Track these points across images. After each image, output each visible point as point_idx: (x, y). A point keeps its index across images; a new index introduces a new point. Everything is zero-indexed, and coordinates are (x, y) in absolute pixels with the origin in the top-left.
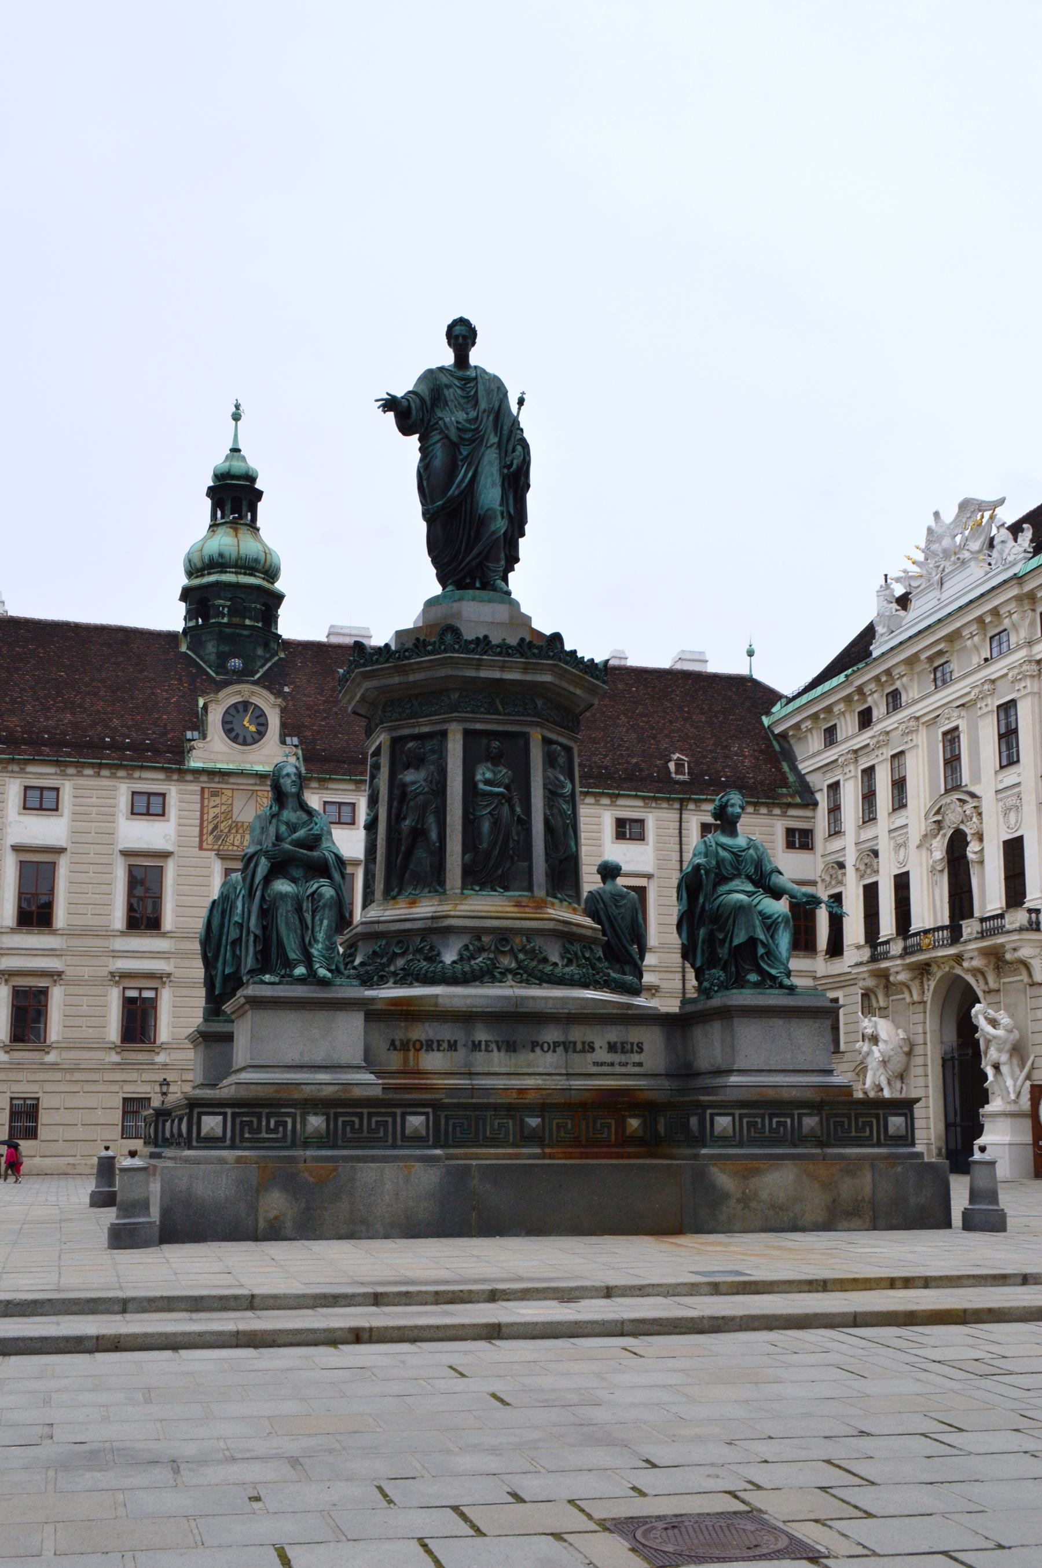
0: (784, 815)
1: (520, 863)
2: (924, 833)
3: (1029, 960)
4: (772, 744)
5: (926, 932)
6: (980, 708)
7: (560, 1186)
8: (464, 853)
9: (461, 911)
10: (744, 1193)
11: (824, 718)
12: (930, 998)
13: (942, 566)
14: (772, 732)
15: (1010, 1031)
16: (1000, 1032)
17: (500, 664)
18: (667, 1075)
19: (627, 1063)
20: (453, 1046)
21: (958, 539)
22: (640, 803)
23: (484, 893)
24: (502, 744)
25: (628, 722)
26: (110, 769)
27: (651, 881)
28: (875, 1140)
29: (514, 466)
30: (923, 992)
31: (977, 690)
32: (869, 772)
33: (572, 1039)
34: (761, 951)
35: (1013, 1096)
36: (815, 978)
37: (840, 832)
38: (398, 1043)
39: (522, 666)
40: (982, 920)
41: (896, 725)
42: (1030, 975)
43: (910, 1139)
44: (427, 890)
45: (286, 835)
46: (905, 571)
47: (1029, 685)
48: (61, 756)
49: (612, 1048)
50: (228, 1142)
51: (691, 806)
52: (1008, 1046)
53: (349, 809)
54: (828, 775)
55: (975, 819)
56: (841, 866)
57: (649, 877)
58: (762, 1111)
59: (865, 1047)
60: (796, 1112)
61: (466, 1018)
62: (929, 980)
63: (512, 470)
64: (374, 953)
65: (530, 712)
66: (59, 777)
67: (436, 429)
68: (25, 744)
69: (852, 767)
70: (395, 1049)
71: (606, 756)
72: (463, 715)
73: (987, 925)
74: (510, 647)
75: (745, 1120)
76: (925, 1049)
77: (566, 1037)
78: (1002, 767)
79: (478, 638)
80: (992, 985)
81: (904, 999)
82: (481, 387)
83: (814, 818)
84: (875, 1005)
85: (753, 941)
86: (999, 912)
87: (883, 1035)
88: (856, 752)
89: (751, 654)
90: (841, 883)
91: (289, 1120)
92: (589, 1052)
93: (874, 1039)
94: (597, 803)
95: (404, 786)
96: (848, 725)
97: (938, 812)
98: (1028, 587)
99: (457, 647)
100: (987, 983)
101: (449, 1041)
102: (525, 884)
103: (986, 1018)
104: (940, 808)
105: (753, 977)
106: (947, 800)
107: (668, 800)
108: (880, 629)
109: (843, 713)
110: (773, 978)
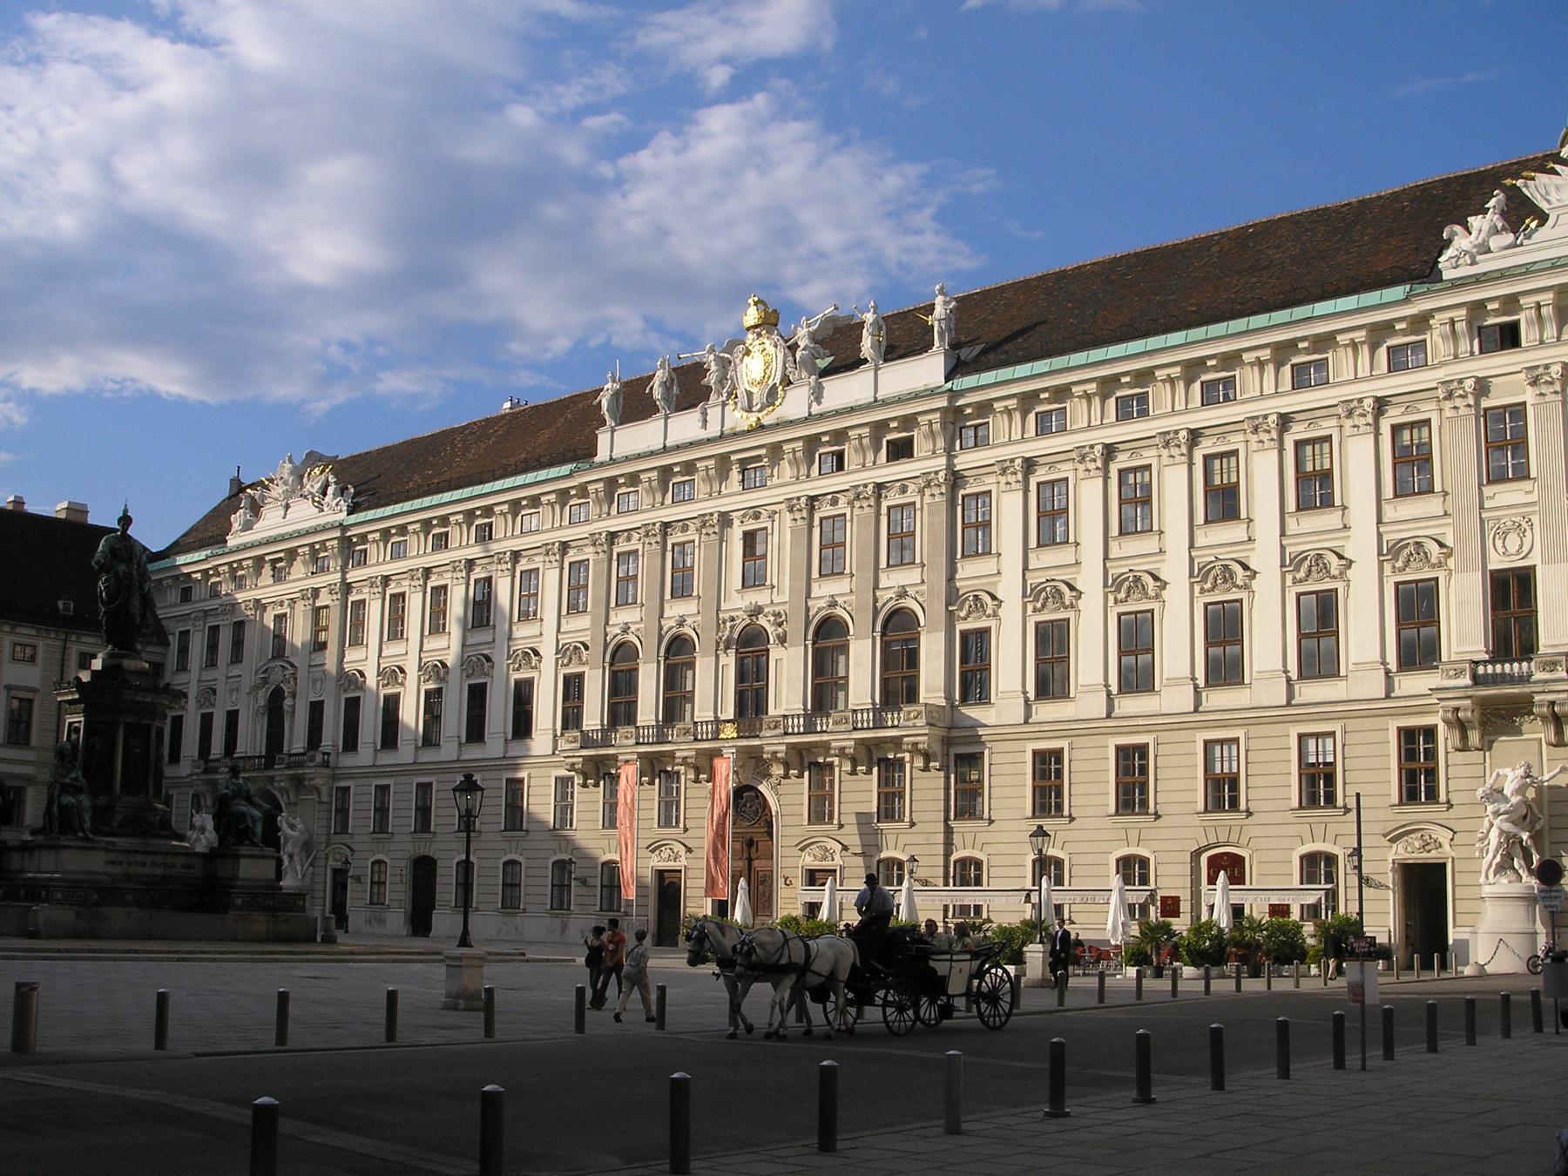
20: (121, 864)
22: (33, 632)
27: (37, 695)
32: (214, 630)
35: (300, 877)
42: (320, 797)
49: (183, 866)
51: (73, 638)
52: (301, 843)
54: (182, 623)
55: (292, 682)
78: (314, 650)
86: (302, 751)
88: (205, 612)
90: (183, 708)
93: (203, 830)
100: (289, 798)
103: (287, 823)
105: (247, 842)
106: (272, 664)
108: (236, 526)
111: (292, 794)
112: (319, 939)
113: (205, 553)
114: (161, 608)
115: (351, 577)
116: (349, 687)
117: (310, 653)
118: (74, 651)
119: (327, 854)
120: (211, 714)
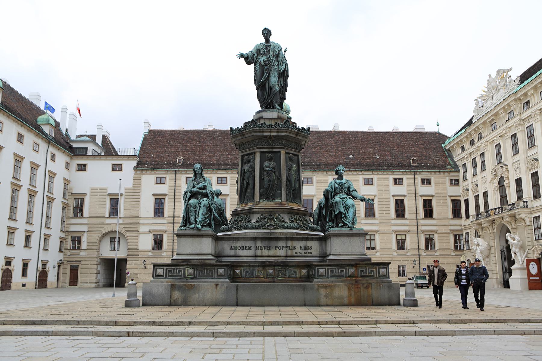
0: (449, 175)
1: (278, 191)
2: (491, 178)
3: (524, 218)
4: (445, 153)
5: (492, 210)
6: (506, 137)
7: (265, 291)
8: (260, 189)
9: (258, 207)
10: (326, 293)
11: (460, 143)
12: (495, 232)
13: (492, 92)
14: (445, 149)
15: (519, 241)
16: (516, 242)
17: (269, 130)
18: (320, 257)
19: (307, 253)
20: (250, 248)
21: (497, 82)
22: (401, 173)
23: (266, 201)
24: (272, 155)
25: (398, 149)
26: (231, 171)
27: (406, 198)
28: (375, 276)
29: (282, 70)
30: (493, 230)
31: (504, 131)
32: (474, 159)
33: (288, 246)
34: (343, 216)
35: (521, 263)
36: (461, 226)
37: (467, 179)
38: (233, 247)
39: (276, 131)
40: (509, 205)
41: (481, 144)
43: (388, 276)
44: (250, 201)
45: (196, 185)
46: (481, 95)
47: (520, 128)
48: (227, 168)
50: (165, 277)
51: (418, 173)
52: (518, 246)
53: (311, 179)
54: (463, 162)
55: (506, 173)
56: (468, 190)
57: (405, 196)
58: (335, 267)
59: (475, 248)
60: (347, 267)
61: (255, 239)
62: (495, 225)
63: (281, 71)
64: (235, 220)
65: (281, 144)
66: (227, 174)
67: (258, 62)
68: (217, 165)
69: (469, 159)
70: (232, 249)
71: (390, 159)
72: (260, 147)
73: (512, 206)
74: (272, 125)
75: (329, 270)
76: (495, 248)
77: (286, 245)
79: (262, 123)
80: (514, 227)
81: (487, 232)
82: (272, 48)
83: (459, 175)
84: (479, 234)
85: (340, 213)
87: (481, 244)
88: (470, 153)
89: (438, 125)
90: (468, 195)
91: (183, 270)
92: (294, 249)
93: (478, 245)
94: (387, 174)
95: (244, 170)
96: (467, 145)
97: (495, 171)
98: (518, 96)
99: (255, 126)
101: (249, 247)
102: (279, 198)
103: (511, 237)
104: (496, 170)
105: (340, 225)
107: (410, 172)
109: (466, 142)
110: (347, 225)
111: (513, 224)
112: (402, 303)
113: (464, 129)
114: (455, 157)
115: (524, 116)
116: (532, 168)
117: (512, 157)
118: (419, 178)
119: (533, 251)
120: (478, 195)
